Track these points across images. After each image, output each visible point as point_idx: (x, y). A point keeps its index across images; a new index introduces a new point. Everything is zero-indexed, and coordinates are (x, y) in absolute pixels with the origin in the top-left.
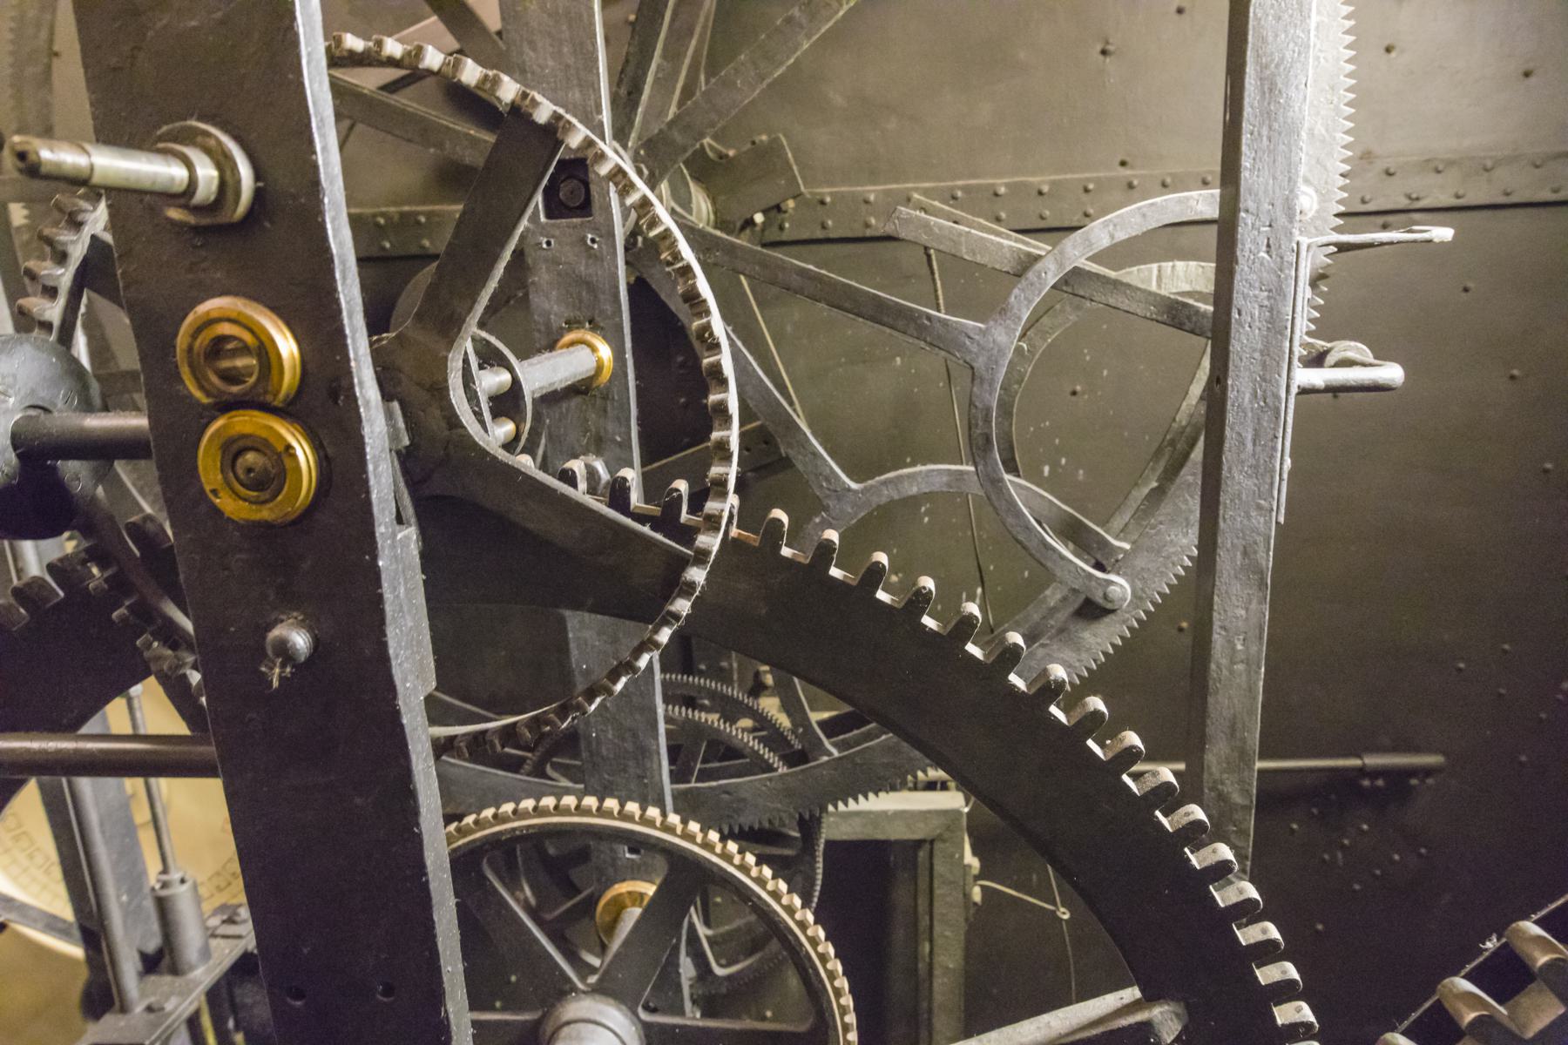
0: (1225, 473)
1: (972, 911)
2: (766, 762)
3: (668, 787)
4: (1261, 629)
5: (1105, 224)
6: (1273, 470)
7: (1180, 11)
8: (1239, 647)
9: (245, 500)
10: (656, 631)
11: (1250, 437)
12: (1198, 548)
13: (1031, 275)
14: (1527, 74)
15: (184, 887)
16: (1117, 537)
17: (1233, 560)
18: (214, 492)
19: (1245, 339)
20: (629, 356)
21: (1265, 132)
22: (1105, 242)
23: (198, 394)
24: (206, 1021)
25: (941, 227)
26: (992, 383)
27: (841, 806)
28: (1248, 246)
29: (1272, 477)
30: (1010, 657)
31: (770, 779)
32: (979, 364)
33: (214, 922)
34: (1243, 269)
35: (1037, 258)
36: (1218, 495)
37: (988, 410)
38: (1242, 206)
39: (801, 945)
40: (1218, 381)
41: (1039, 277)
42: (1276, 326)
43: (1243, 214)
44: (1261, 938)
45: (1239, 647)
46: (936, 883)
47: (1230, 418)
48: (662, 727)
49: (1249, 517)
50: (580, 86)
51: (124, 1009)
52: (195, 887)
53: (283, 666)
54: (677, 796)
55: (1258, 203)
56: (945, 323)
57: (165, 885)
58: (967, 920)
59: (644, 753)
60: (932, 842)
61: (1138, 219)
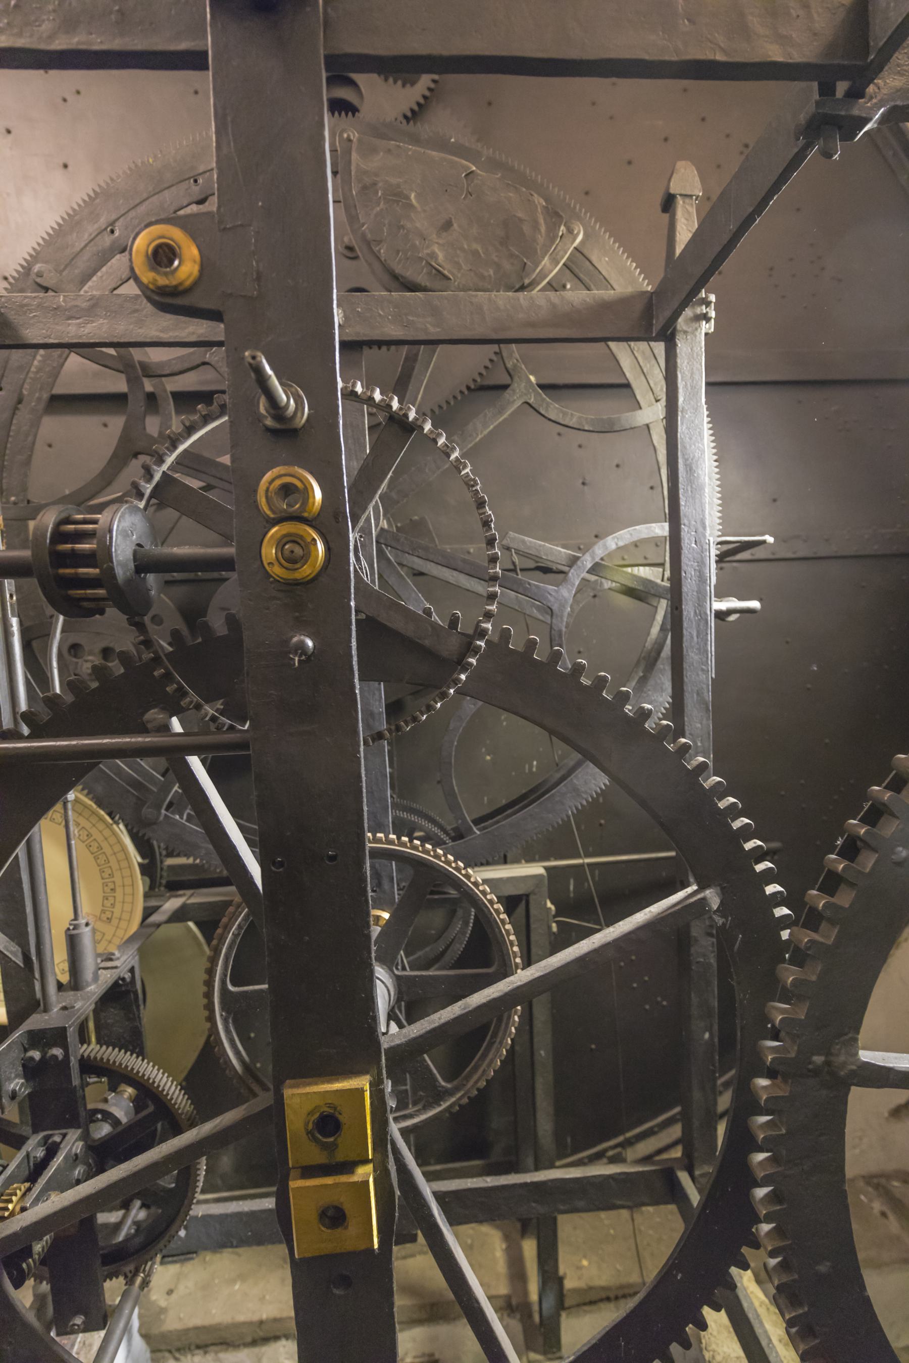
0: (685, 652)
1: (553, 938)
2: (442, 839)
4: (709, 734)
5: (613, 538)
6: (707, 651)
7: (618, 466)
8: (699, 744)
9: (287, 568)
11: (695, 634)
12: (672, 697)
13: (579, 563)
15: (88, 929)
17: (693, 697)
18: (269, 564)
19: (689, 586)
21: (689, 489)
22: (614, 547)
23: (268, 512)
24: (91, 1025)
25: (530, 542)
26: (562, 617)
28: (686, 541)
30: (625, 697)
32: (555, 608)
33: (99, 960)
34: (685, 552)
35: (578, 558)
36: (682, 664)
37: (560, 631)
39: (492, 914)
40: (677, 608)
42: (702, 579)
44: (754, 845)
45: (699, 744)
46: (532, 920)
47: (685, 625)
49: (698, 675)
50: (357, 459)
51: (46, 1010)
52: (94, 931)
53: (300, 656)
55: (689, 521)
56: (537, 586)
57: (76, 927)
58: (550, 943)
60: (527, 896)
61: (629, 536)
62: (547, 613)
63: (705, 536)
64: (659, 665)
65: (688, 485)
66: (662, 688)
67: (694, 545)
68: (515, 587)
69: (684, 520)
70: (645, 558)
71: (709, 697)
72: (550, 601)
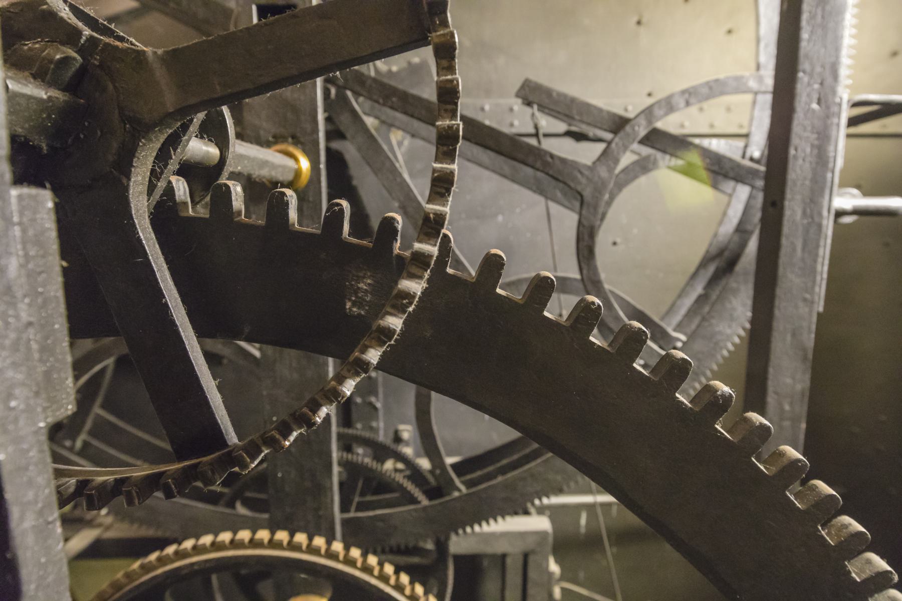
0: (781, 270)
3: (338, 516)
8: (787, 407)
10: (364, 351)
13: (628, 128)
14: (895, 54)
16: (675, 330)
20: (322, 166)
27: (468, 529)
29: (815, 277)
31: (415, 510)
32: (587, 193)
38: (801, 67)
40: (774, 204)
41: (634, 130)
42: (822, 160)
43: (800, 75)
48: (336, 469)
54: (345, 522)
59: (320, 490)
62: (576, 198)
63: (834, 92)
64: (732, 282)
65: (817, 6)
66: (731, 315)
67: (815, 106)
68: (530, 160)
69: (804, 65)
70: (712, 126)
71: (809, 340)
72: (580, 183)
